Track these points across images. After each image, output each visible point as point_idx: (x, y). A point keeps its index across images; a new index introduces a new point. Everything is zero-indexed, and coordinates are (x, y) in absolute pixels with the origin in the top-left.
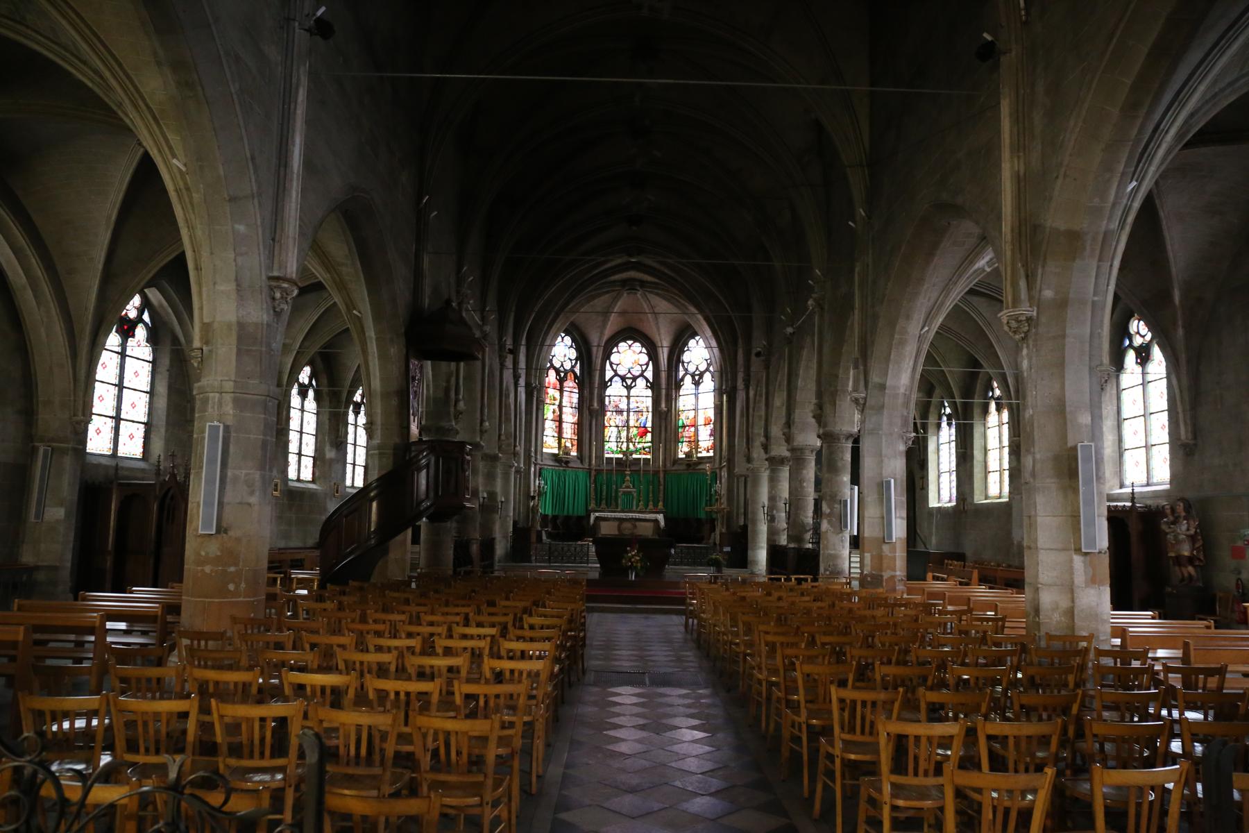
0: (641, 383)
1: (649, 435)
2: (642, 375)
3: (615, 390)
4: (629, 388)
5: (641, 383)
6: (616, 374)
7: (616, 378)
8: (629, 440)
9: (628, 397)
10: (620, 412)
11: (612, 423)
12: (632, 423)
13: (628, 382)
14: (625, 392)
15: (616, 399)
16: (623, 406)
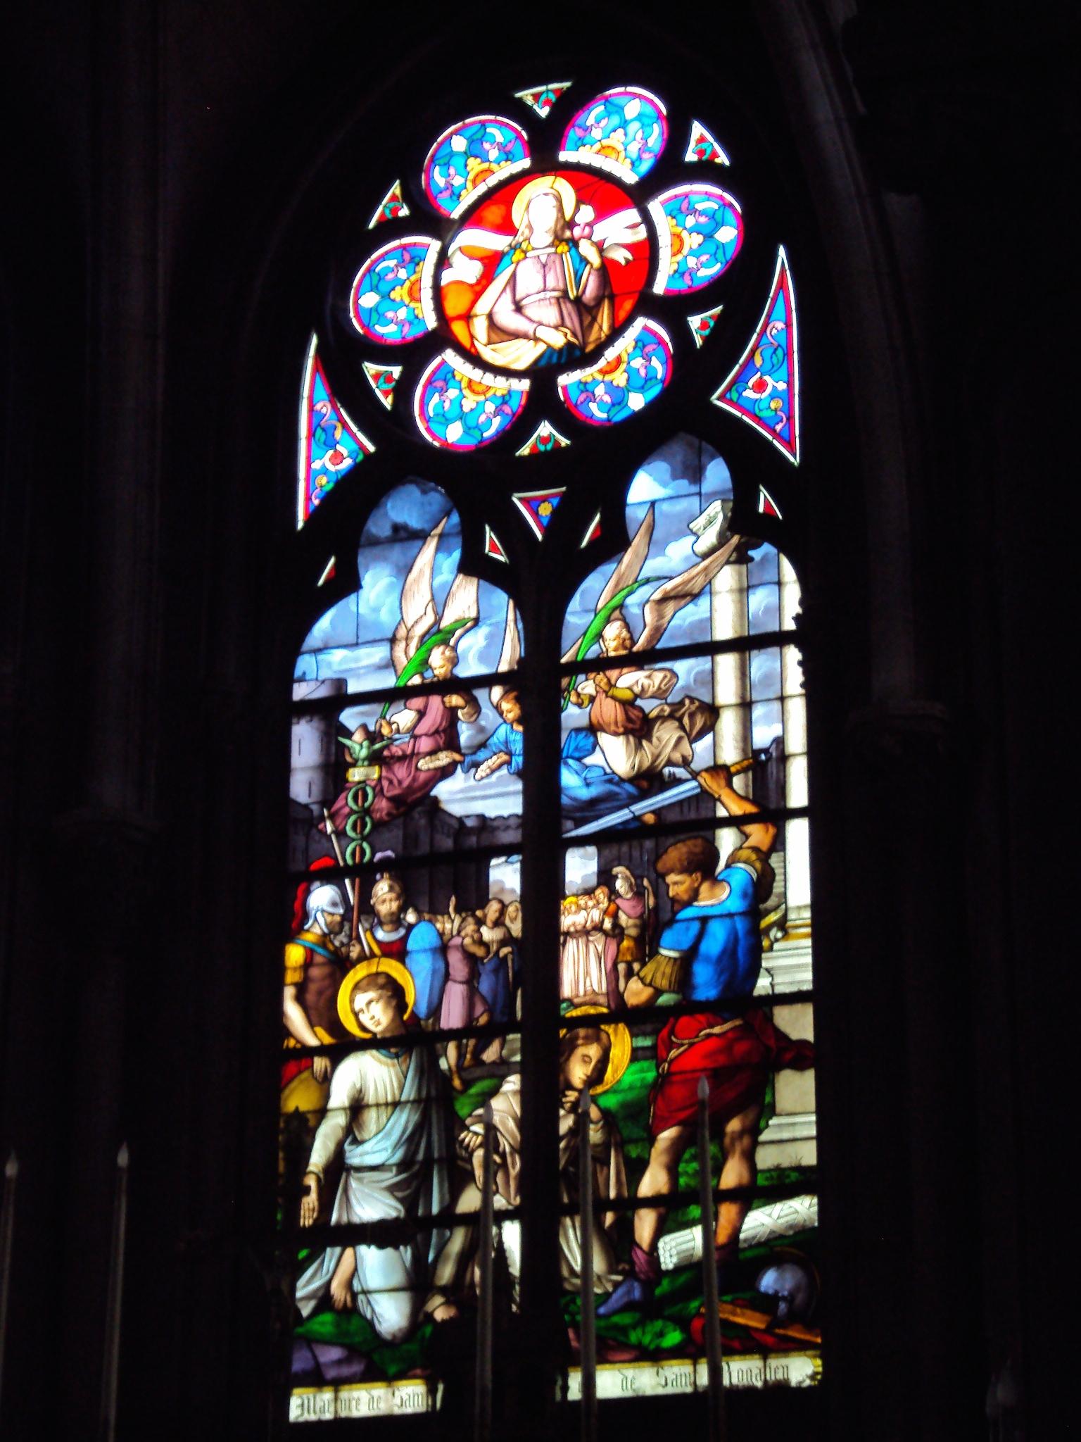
0: (675, 515)
1: (794, 1123)
2: (685, 418)
3: (412, 612)
4: (539, 582)
5: (675, 515)
6: (398, 453)
7: (406, 506)
8: (552, 1181)
9: (539, 681)
10: (439, 861)
11: (366, 1010)
12: (582, 973)
13: (540, 508)
14: (490, 636)
15: (404, 717)
16: (483, 794)
